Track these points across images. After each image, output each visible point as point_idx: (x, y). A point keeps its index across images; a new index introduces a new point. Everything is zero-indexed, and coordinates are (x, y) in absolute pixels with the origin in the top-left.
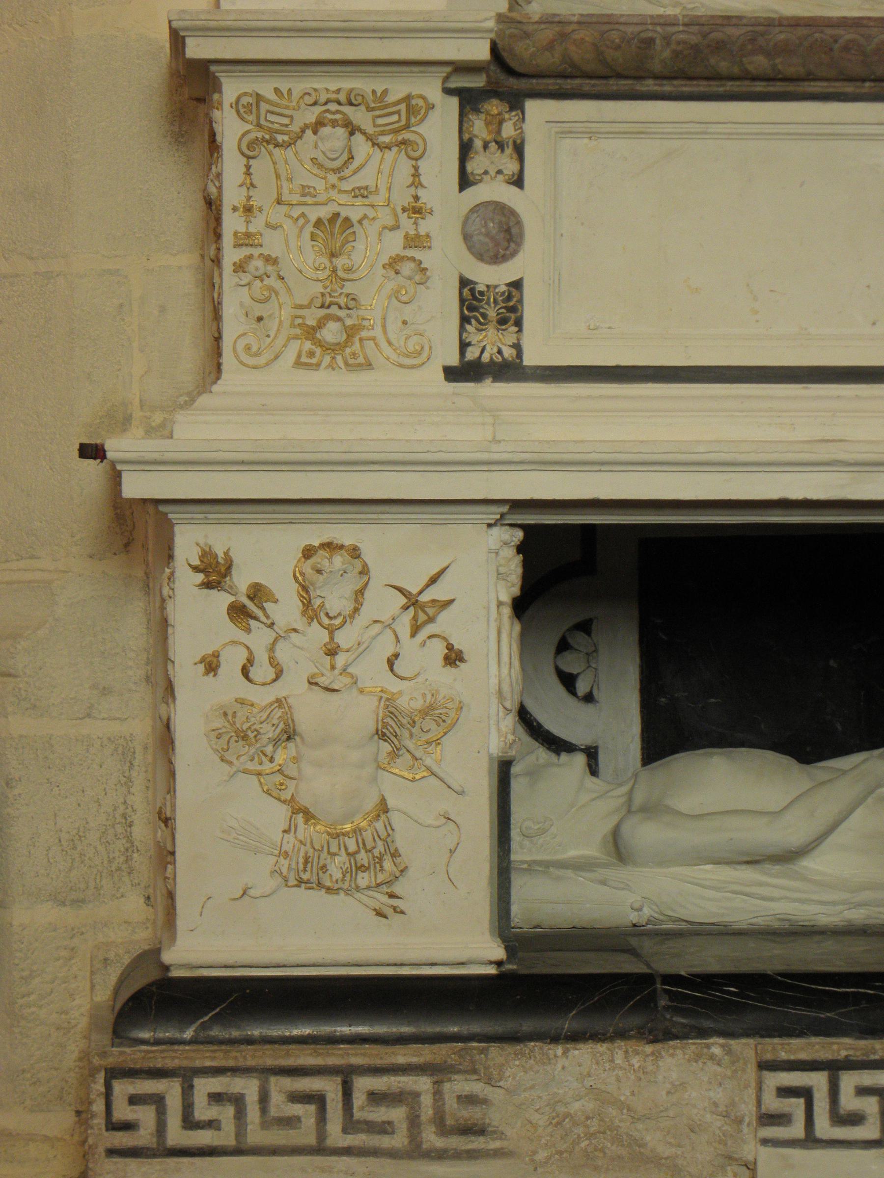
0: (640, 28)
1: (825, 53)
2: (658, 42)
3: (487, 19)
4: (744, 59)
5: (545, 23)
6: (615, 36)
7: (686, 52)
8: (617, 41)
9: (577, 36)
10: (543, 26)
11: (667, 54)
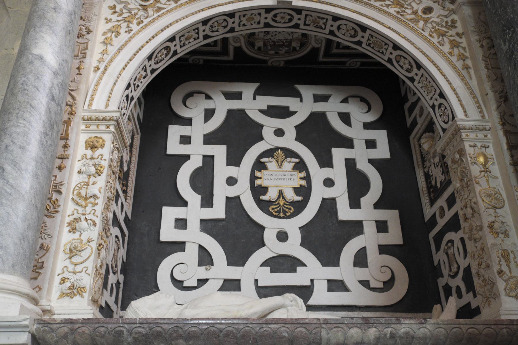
0: (115, 326)
1: (216, 338)
2: (125, 332)
3: (24, 320)
4: (172, 342)
5: (63, 323)
6: (102, 329)
7: (140, 338)
8: (103, 332)
9: (79, 330)
10: (62, 325)
11: (130, 339)
